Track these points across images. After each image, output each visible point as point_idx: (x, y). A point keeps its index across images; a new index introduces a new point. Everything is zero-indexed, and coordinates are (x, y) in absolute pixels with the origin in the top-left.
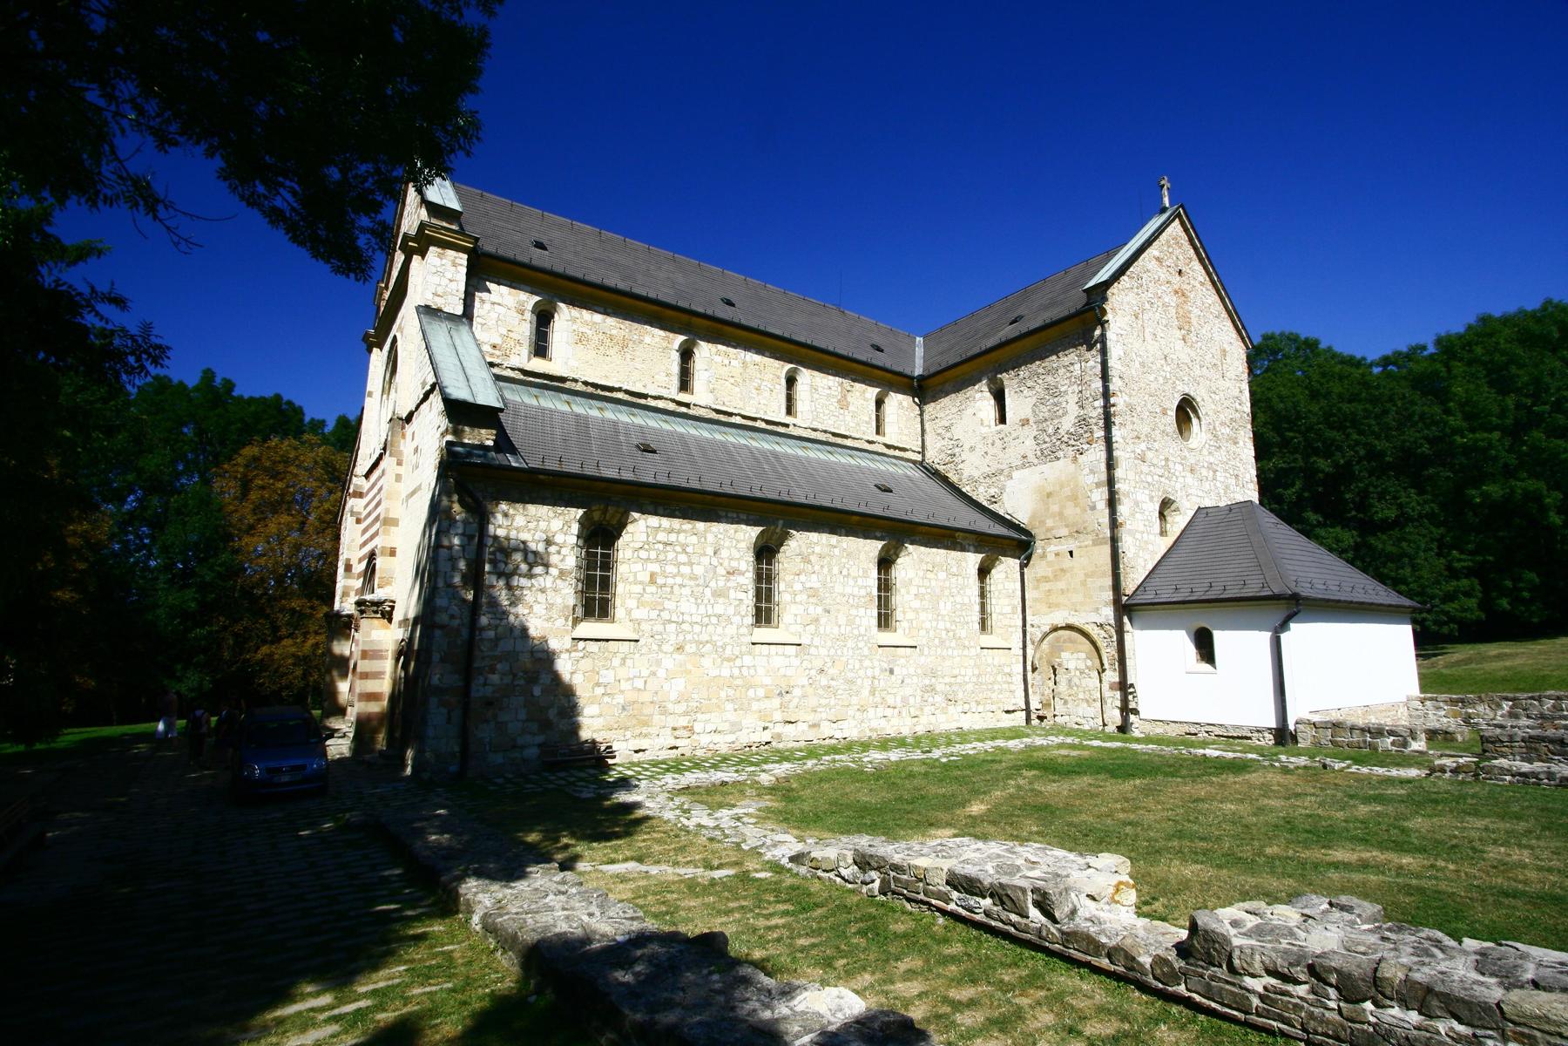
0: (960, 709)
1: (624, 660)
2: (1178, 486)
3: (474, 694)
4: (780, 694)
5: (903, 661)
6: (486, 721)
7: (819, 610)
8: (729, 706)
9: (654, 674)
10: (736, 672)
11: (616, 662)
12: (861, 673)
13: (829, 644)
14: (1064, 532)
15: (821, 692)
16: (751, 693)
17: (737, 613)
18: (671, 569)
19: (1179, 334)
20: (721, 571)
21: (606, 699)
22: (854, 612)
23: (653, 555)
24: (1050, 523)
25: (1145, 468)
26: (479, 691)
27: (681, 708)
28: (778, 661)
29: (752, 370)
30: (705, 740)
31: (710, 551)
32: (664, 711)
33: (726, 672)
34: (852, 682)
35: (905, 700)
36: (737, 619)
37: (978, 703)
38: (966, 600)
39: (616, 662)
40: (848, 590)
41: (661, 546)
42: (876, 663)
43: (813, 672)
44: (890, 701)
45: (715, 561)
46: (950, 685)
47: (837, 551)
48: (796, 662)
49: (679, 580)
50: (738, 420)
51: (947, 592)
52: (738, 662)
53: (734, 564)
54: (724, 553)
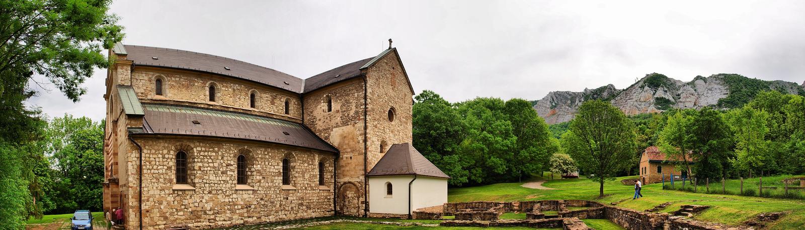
0: (312, 211)
1: (191, 196)
4: (247, 207)
5: (291, 195)
6: (147, 217)
7: (261, 177)
8: (229, 212)
9: (201, 201)
10: (231, 200)
11: (188, 197)
12: (277, 199)
13: (264, 189)
14: (349, 150)
15: (262, 206)
16: (236, 207)
17: (230, 179)
18: (206, 165)
21: (185, 210)
22: (273, 178)
23: (199, 160)
24: (345, 147)
26: (144, 207)
27: (211, 212)
28: (245, 196)
29: (237, 92)
30: (220, 223)
31: (220, 158)
32: (205, 213)
33: (227, 200)
34: (272, 203)
35: (292, 208)
36: (230, 182)
37: (318, 209)
38: (315, 173)
39: (188, 197)
40: (271, 170)
41: (202, 157)
42: (282, 196)
43: (259, 199)
44: (287, 209)
45: (222, 161)
46: (308, 203)
47: (267, 156)
48: (252, 196)
49: (209, 169)
50: (232, 110)
51: (308, 171)
53: (229, 162)
54: (225, 158)
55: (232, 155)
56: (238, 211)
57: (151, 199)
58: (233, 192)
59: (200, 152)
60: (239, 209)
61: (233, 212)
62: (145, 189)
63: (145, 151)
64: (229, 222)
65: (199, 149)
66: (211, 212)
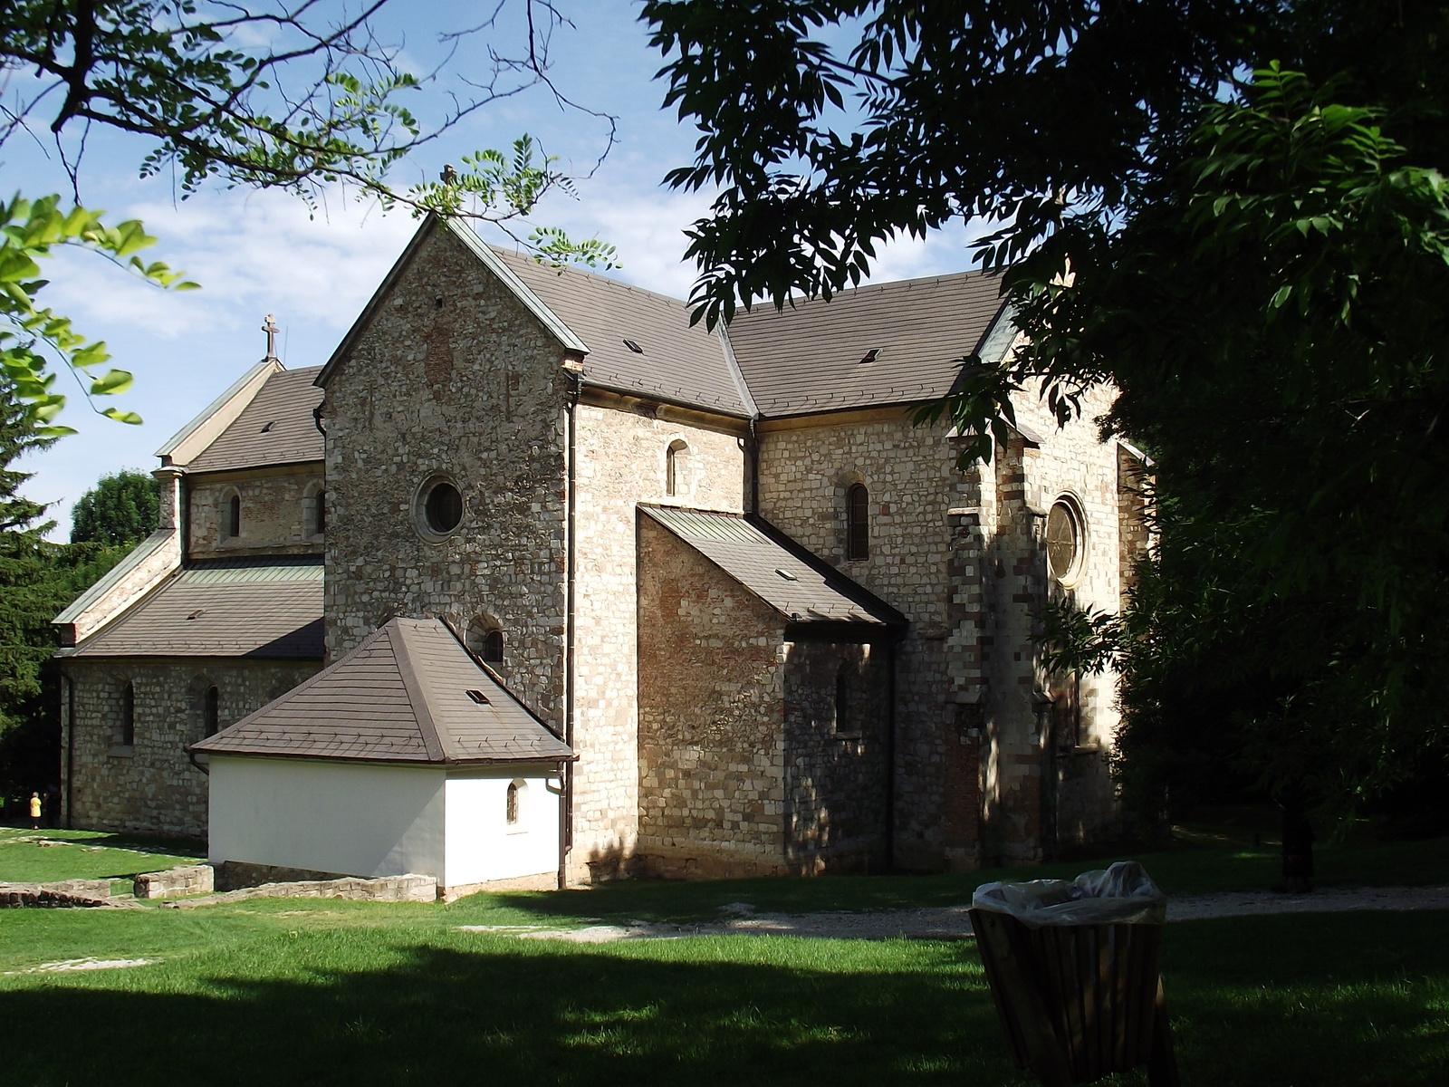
2: (409, 596)
3: (74, 786)
8: (178, 807)
11: (125, 771)
19: (426, 394)
20: (172, 710)
25: (360, 587)
27: (153, 804)
30: (166, 827)
31: (166, 696)
32: (146, 805)
49: (151, 718)
52: (181, 776)
53: (179, 705)
54: (174, 697)
55: (183, 690)
56: (191, 808)
57: (83, 771)
58: (185, 766)
59: (140, 685)
60: (193, 804)
61: (185, 808)
62: (78, 753)
63: (80, 686)
64: (178, 828)
65: (139, 680)
66: (153, 804)
